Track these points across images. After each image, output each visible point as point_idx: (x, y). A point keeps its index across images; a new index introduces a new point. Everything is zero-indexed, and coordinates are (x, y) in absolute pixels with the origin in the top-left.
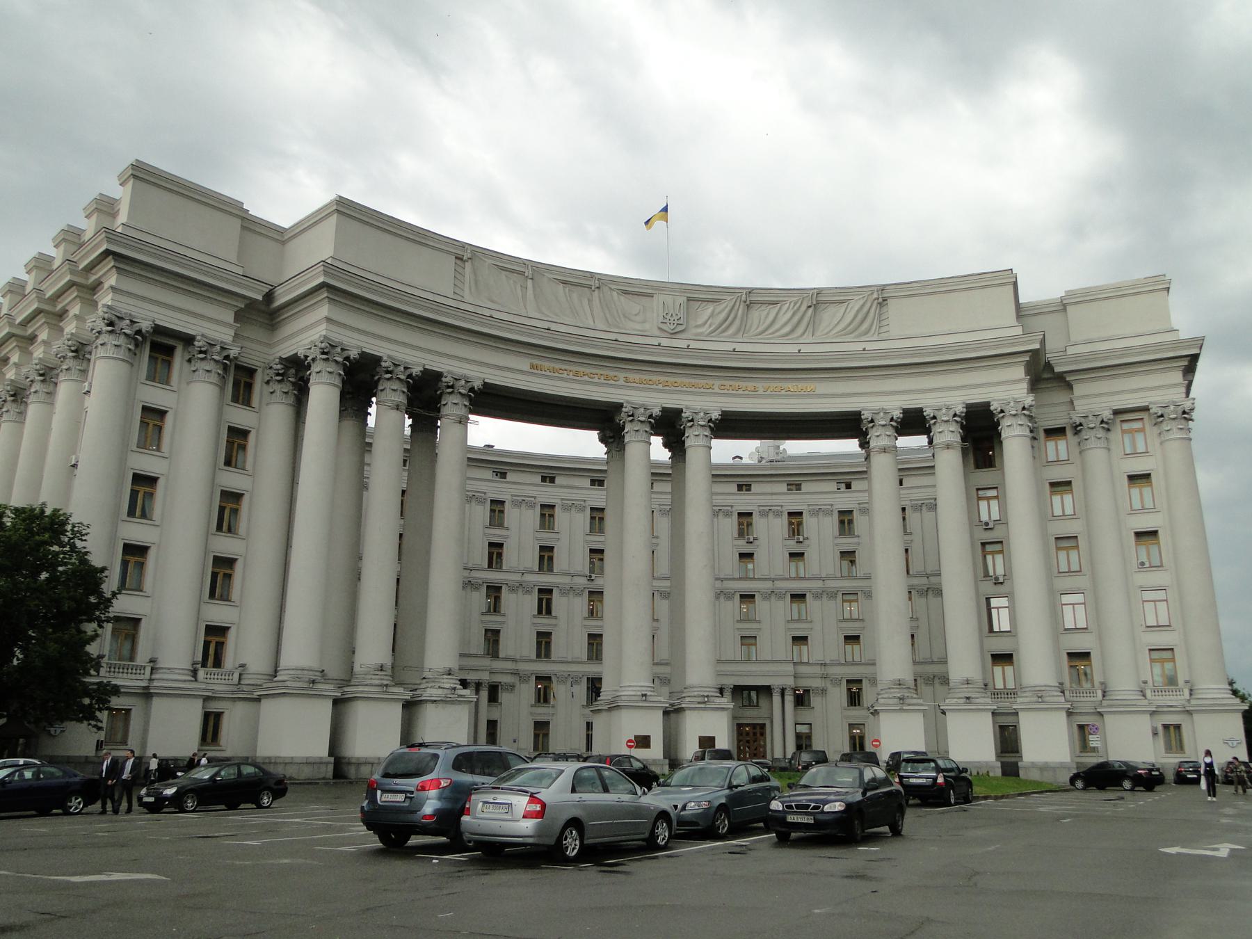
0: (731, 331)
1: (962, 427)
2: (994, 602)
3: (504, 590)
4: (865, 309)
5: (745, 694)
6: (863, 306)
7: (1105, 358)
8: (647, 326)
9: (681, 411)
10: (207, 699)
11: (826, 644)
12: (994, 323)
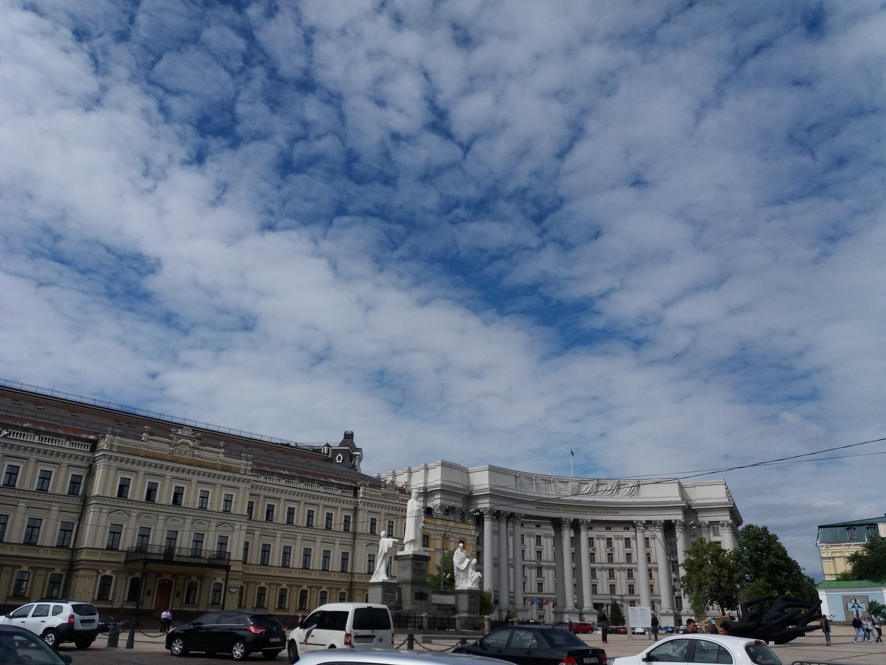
5: (597, 606)
11: (622, 589)
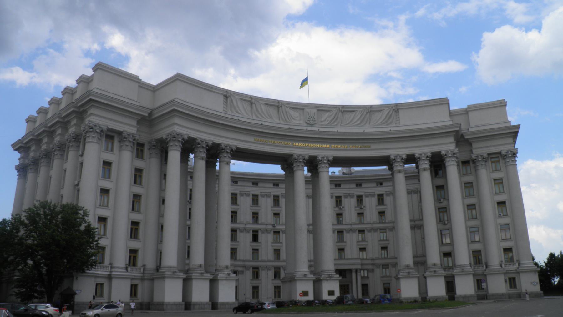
0: (335, 124)
1: (430, 161)
2: (443, 232)
3: (238, 231)
4: (390, 114)
5: (341, 272)
6: (389, 113)
7: (484, 133)
8: (302, 122)
9: (315, 157)
10: (132, 279)
11: (374, 251)
12: (440, 120)
